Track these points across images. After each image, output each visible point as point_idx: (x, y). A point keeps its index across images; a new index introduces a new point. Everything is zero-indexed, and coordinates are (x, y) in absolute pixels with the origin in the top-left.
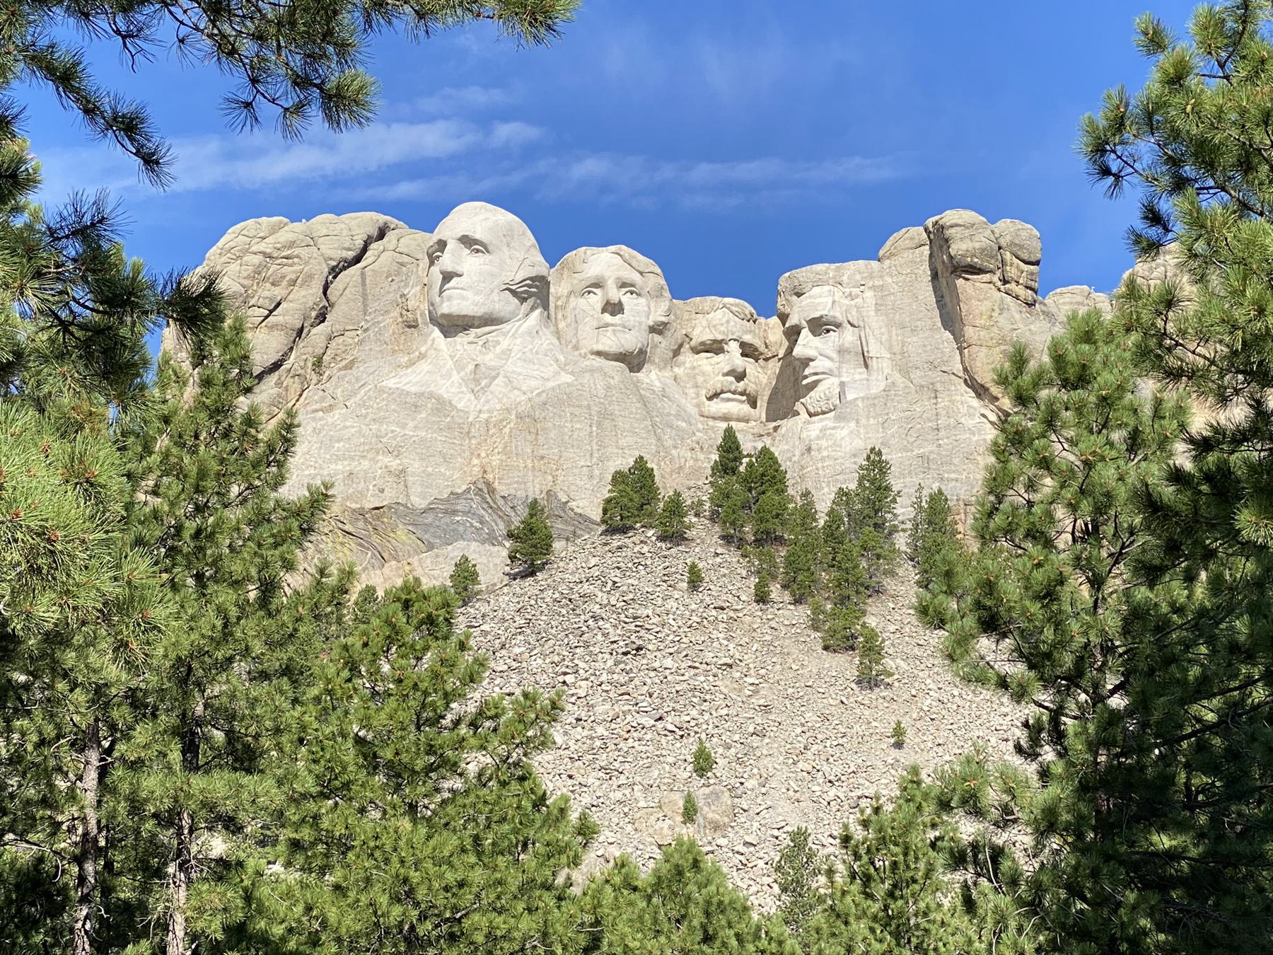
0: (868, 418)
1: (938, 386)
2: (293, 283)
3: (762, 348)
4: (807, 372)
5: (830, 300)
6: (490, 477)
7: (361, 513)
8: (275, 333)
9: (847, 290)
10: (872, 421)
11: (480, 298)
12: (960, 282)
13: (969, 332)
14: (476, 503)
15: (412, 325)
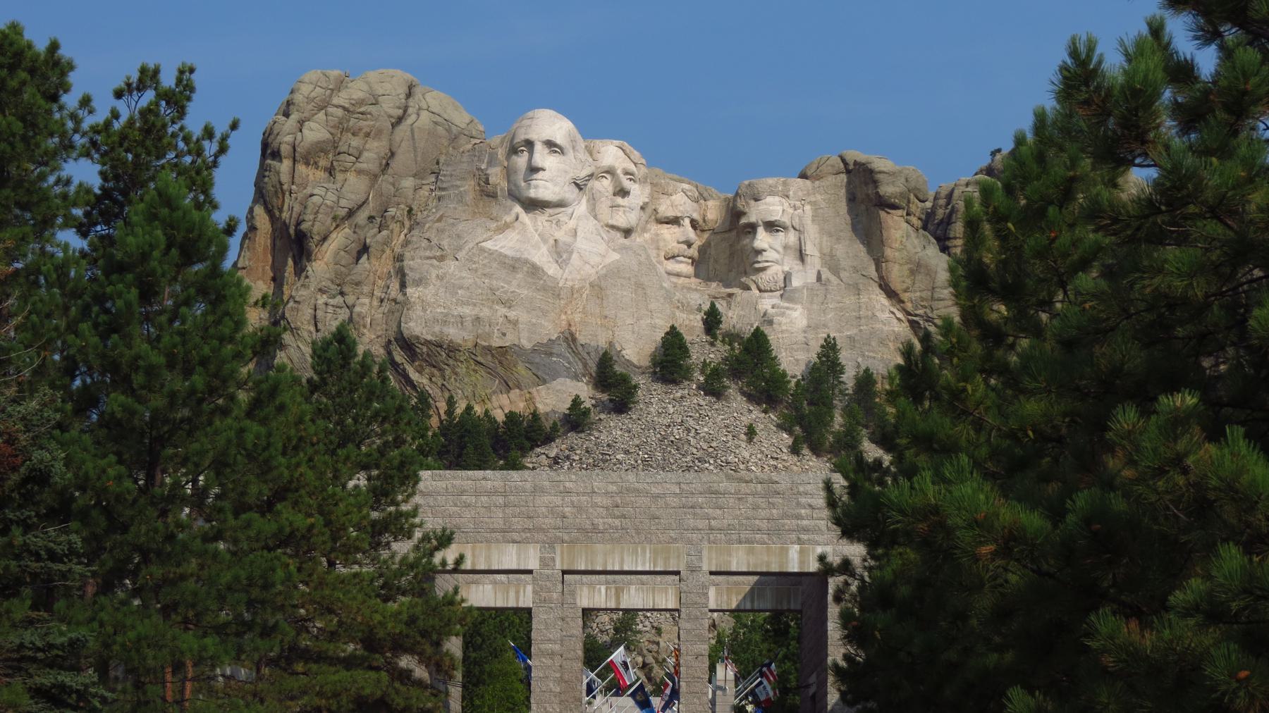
0: (812, 303)
1: (861, 287)
2: (368, 135)
3: (701, 222)
4: (760, 258)
5: (779, 208)
6: (573, 329)
7: (489, 349)
8: (363, 177)
9: (792, 202)
10: (815, 306)
11: (557, 189)
12: (882, 214)
13: (888, 252)
14: (563, 348)
15: (493, 196)
